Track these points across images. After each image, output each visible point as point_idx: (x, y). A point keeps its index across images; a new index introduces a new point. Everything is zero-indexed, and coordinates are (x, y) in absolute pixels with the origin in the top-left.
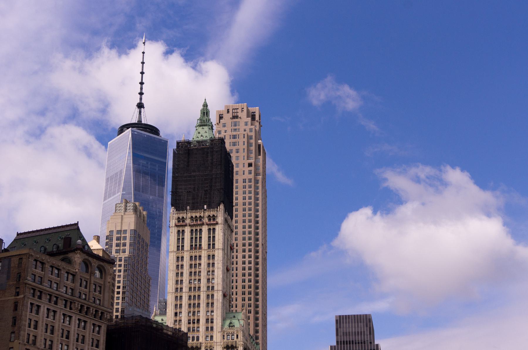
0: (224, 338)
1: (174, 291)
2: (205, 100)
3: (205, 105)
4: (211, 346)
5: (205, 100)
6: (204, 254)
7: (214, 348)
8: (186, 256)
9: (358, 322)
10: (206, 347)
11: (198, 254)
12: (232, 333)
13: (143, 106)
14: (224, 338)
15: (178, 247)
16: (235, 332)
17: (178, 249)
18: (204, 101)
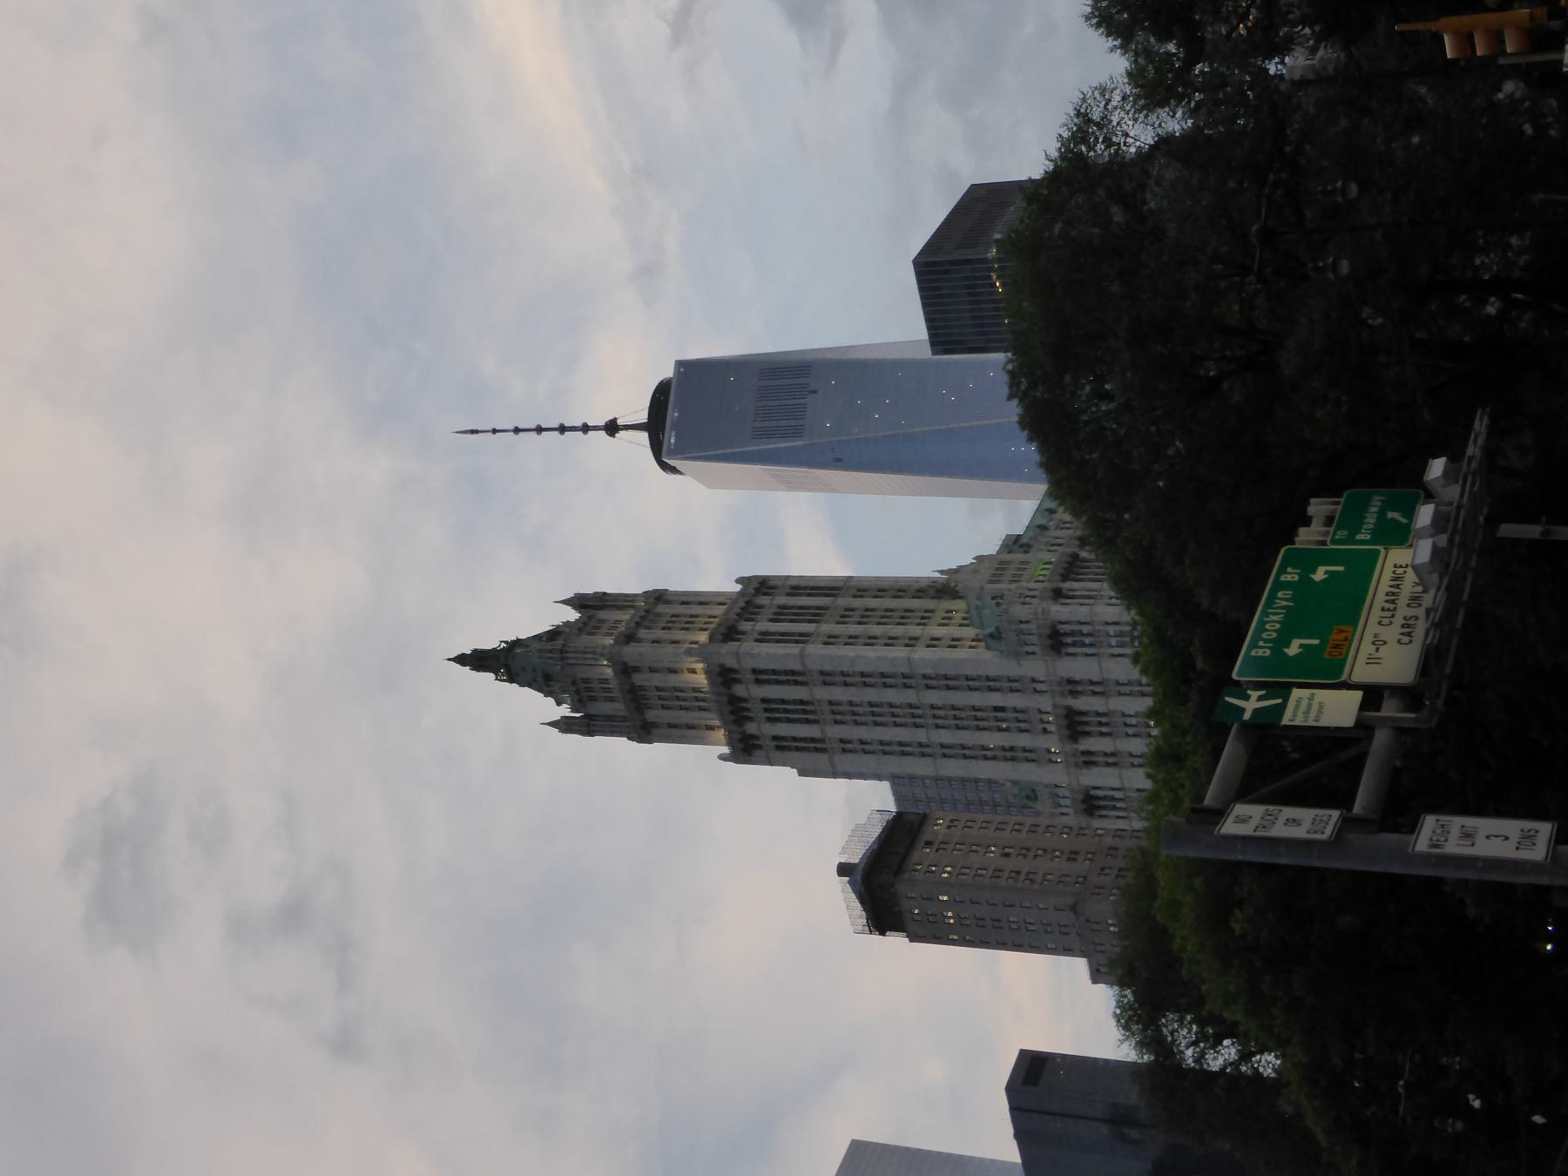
0: (1034, 653)
1: (929, 760)
2: (449, 659)
3: (461, 660)
4: (1060, 684)
5: (449, 659)
6: (822, 693)
7: (1062, 678)
8: (835, 732)
9: (941, 296)
10: (1062, 694)
11: (828, 708)
12: (1016, 635)
13: (611, 421)
14: (1034, 653)
15: (816, 750)
16: (1013, 627)
17: (823, 750)
18: (451, 663)
